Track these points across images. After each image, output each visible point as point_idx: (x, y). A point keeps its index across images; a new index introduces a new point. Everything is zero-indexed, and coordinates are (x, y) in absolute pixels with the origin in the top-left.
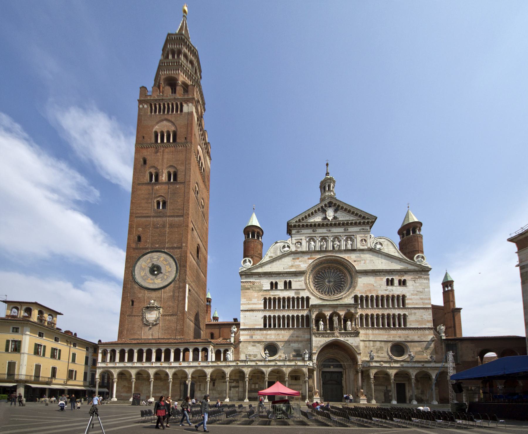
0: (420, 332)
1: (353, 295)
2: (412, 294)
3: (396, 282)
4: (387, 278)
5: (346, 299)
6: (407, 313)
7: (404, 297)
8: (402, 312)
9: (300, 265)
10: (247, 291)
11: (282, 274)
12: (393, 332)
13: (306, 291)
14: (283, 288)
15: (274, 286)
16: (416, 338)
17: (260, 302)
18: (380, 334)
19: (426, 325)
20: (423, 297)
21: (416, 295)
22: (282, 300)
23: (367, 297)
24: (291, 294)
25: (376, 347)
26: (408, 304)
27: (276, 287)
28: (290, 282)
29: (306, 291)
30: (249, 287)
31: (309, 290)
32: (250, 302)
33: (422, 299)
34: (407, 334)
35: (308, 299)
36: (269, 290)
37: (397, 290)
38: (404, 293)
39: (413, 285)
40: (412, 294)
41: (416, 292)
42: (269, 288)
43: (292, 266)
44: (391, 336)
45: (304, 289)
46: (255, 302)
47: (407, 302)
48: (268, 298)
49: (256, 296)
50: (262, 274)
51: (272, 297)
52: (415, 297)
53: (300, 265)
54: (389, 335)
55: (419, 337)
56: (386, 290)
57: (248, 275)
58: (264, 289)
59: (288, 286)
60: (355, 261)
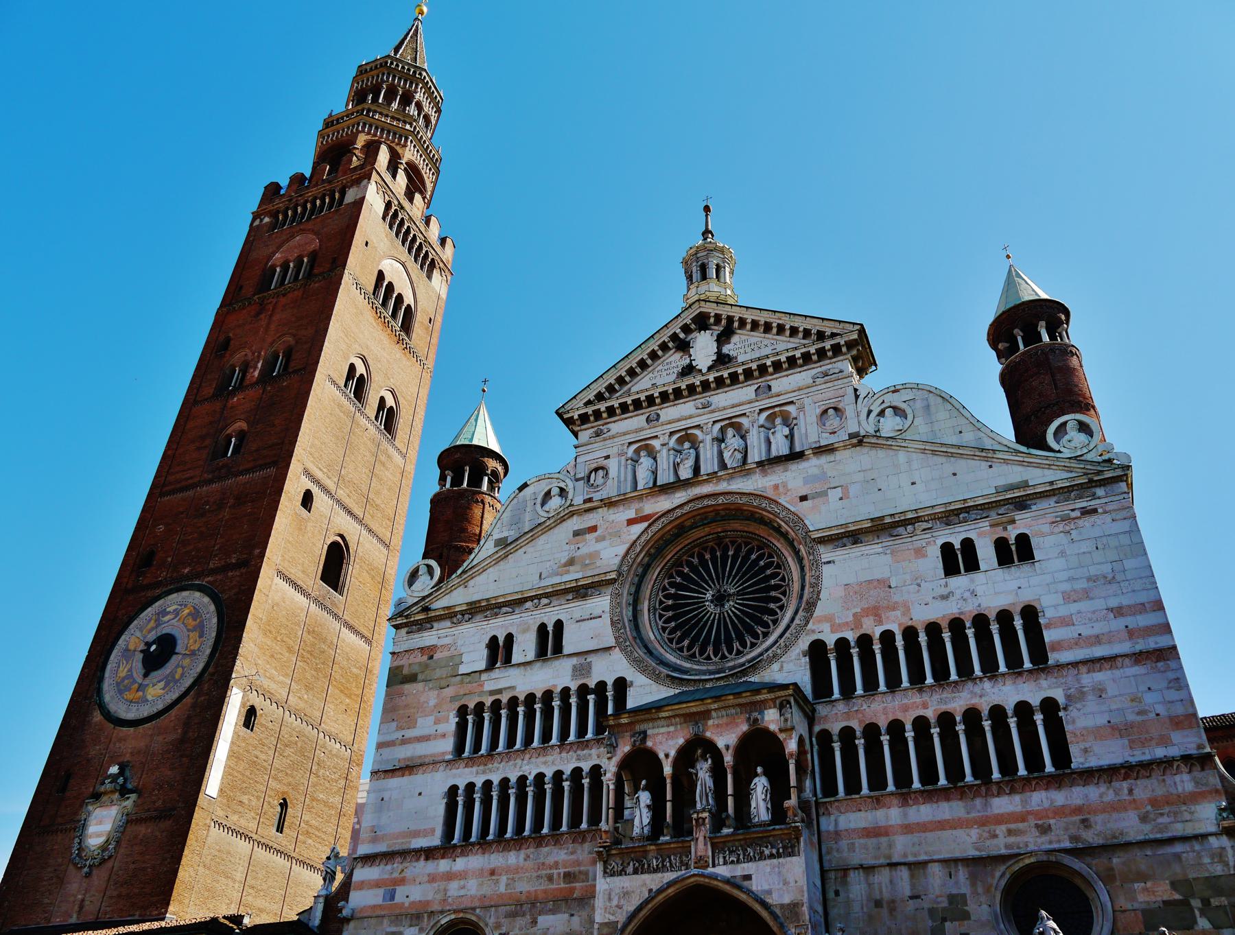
0: (1145, 789)
1: (804, 643)
2: (1068, 598)
3: (986, 553)
4: (940, 542)
5: (776, 666)
6: (1059, 695)
7: (1030, 613)
8: (1032, 692)
10: (407, 686)
11: (531, 598)
12: (1003, 804)
14: (531, 656)
15: (499, 652)
16: (1131, 826)
18: (941, 825)
19: (1165, 741)
20: (1126, 601)
21: (1086, 595)
22: (521, 709)
23: (865, 641)
24: (556, 676)
25: (926, 905)
26: (1058, 646)
27: (508, 660)
28: (559, 625)
29: (617, 654)
30: (416, 669)
33: (1118, 612)
34: (1078, 810)
35: (621, 685)
36: (481, 672)
37: (993, 590)
38: (1027, 597)
39: (1062, 554)
42: (482, 665)
43: (571, 562)
44: (1001, 830)
45: (608, 649)
46: (426, 732)
47: (1049, 636)
48: (471, 706)
49: (432, 703)
50: (463, 613)
51: (488, 701)
52: (1084, 606)
54: (982, 822)
55: (1144, 819)
56: (945, 597)
57: (416, 623)
58: (463, 669)
59: (550, 642)
60: (803, 498)
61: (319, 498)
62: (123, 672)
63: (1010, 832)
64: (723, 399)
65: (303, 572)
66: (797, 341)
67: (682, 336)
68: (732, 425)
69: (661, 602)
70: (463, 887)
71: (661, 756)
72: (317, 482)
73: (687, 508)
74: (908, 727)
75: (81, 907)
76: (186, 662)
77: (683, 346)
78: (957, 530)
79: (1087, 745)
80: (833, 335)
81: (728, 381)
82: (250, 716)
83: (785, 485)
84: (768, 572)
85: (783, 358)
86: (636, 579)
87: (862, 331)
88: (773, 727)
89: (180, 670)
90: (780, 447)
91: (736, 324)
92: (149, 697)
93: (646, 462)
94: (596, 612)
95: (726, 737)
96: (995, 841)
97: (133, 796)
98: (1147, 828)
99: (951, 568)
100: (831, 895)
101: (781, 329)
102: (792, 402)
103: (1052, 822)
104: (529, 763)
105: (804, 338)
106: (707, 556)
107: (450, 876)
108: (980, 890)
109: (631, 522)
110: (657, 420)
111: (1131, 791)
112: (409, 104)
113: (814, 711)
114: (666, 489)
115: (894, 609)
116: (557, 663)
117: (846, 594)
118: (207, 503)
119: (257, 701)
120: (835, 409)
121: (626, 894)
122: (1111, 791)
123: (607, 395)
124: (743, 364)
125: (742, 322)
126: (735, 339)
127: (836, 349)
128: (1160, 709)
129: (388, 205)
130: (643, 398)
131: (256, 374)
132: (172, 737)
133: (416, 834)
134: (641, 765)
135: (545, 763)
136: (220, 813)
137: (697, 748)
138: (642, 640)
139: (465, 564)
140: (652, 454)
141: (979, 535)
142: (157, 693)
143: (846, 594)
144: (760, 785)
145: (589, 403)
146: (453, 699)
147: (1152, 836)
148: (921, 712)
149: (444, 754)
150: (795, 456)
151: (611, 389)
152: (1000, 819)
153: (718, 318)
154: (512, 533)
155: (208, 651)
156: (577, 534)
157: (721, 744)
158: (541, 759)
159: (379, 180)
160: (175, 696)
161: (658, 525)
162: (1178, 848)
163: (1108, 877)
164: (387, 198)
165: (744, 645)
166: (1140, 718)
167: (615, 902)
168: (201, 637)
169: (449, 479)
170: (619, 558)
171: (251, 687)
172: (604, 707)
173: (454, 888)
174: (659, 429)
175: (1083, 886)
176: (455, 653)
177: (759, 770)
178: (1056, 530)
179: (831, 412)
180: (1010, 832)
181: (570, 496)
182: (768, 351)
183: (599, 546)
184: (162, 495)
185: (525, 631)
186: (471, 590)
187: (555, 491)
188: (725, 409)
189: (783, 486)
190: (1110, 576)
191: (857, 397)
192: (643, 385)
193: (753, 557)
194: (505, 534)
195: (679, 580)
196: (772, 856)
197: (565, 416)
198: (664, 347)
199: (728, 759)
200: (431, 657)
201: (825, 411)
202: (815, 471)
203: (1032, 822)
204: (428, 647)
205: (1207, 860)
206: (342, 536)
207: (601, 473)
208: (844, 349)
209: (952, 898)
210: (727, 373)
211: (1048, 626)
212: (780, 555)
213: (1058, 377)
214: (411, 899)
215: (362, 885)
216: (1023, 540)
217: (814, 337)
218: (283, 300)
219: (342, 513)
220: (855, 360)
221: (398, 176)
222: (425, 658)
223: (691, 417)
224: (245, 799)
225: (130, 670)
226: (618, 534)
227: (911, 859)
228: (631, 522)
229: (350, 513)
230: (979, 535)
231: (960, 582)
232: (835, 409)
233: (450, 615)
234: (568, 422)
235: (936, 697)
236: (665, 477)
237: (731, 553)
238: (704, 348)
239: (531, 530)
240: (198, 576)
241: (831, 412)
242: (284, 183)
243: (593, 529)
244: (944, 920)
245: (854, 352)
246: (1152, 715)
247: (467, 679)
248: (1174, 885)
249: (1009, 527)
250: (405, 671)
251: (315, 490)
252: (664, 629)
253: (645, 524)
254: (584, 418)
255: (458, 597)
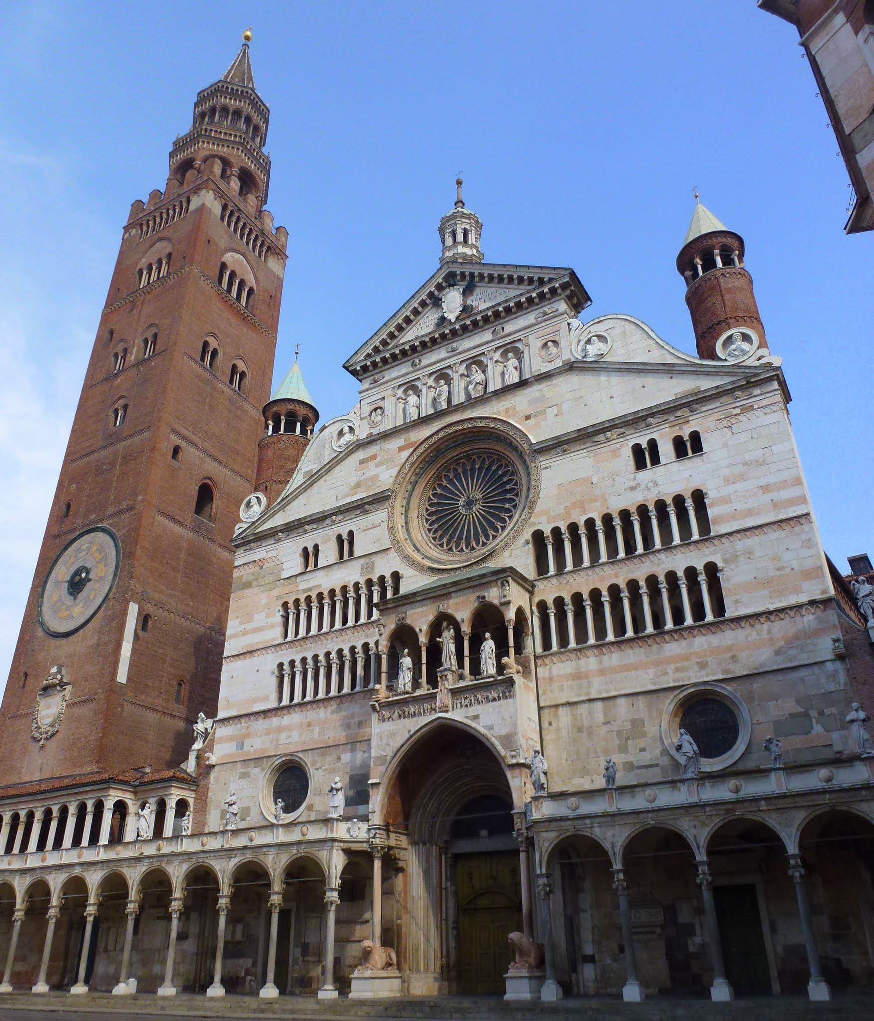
1: (528, 535)
2: (728, 480)
3: (666, 450)
4: (631, 443)
7: (699, 496)
8: (698, 559)
9: (377, 475)
10: (246, 591)
12: (673, 648)
13: (392, 554)
17: (271, 621)
18: (626, 668)
19: (797, 590)
20: (772, 479)
21: (742, 477)
23: (573, 528)
24: (350, 574)
25: (615, 729)
26: (719, 520)
28: (351, 534)
29: (392, 554)
30: (251, 578)
31: (399, 550)
32: (249, 626)
33: (766, 488)
34: (729, 648)
35: (396, 576)
37: (671, 478)
39: (725, 445)
40: (728, 480)
41: (740, 468)
43: (358, 485)
44: (671, 668)
47: (711, 512)
49: (264, 602)
52: (740, 486)
53: (377, 475)
54: (657, 664)
56: (633, 488)
58: (285, 575)
60: (528, 418)
61: (189, 452)
62: (56, 598)
63: (677, 669)
64: (467, 343)
65: (179, 509)
66: (524, 288)
67: (436, 293)
68: (475, 363)
69: (427, 510)
70: (289, 737)
71: (417, 630)
72: (184, 438)
73: (442, 434)
74: (605, 593)
75: (41, 769)
76: (97, 586)
77: (436, 301)
78: (643, 433)
79: (738, 597)
80: (551, 280)
81: (471, 327)
82: (144, 620)
83: (514, 408)
84: (505, 479)
85: (512, 304)
86: (406, 495)
87: (573, 274)
88: (496, 602)
89: (93, 593)
90: (513, 377)
91: (477, 279)
92: (75, 615)
93: (412, 399)
94: (377, 523)
95: (463, 610)
96: (666, 678)
97: (69, 688)
98: (779, 658)
99: (640, 464)
100: (545, 725)
101: (511, 279)
102: (520, 340)
103: (709, 659)
104: (332, 642)
105: (529, 284)
106: (460, 471)
107: (280, 730)
108: (654, 715)
109: (401, 449)
110: (419, 364)
111: (769, 631)
112: (240, 117)
113: (533, 586)
114: (423, 421)
115: (595, 500)
116: (350, 564)
117: (562, 491)
118: (104, 464)
119: (149, 608)
120: (554, 342)
121: (392, 735)
122: (754, 632)
123: (381, 348)
124: (481, 312)
125: (481, 276)
126: (478, 291)
127: (553, 291)
128: (795, 564)
129: (225, 207)
130: (407, 348)
131: (133, 358)
132: (93, 641)
133: (256, 700)
134: (403, 637)
135: (343, 641)
136: (131, 695)
137: (442, 621)
138: (411, 541)
139: (283, 494)
140: (417, 392)
141: (662, 436)
142: (80, 610)
143: (562, 491)
144: (489, 646)
145: (368, 356)
146: (278, 598)
147: (784, 666)
148: (614, 581)
149: (273, 639)
150: (523, 384)
151: (384, 343)
152: (670, 660)
153: (463, 274)
154: (316, 466)
155: (111, 577)
156: (362, 462)
157: (459, 618)
158: (341, 638)
159: (214, 187)
160: (91, 612)
161: (421, 449)
162: (803, 673)
163: (750, 699)
164: (224, 202)
165: (487, 538)
166: (779, 573)
167: (384, 742)
168: (106, 566)
169: (271, 428)
170: (393, 478)
171: (142, 601)
172: (386, 595)
173: (283, 738)
174: (420, 372)
175: (732, 707)
176: (278, 563)
177: (488, 635)
178: (721, 426)
179: (550, 344)
180: (677, 669)
181: (356, 433)
182: (502, 298)
183: (379, 469)
184: (73, 461)
185: (326, 542)
186: (289, 513)
187: (346, 429)
188: (469, 350)
189: (510, 411)
190: (761, 460)
191: (570, 329)
192: (409, 336)
193: (494, 468)
194: (311, 467)
195: (439, 491)
196: (494, 700)
197: (350, 369)
198: (423, 304)
199: (466, 628)
200: (262, 567)
201: (545, 345)
202: (538, 394)
203: (694, 659)
204: (260, 560)
205: (823, 680)
206: (210, 478)
207: (379, 411)
208: (559, 291)
209: (634, 722)
210: (472, 323)
211: (712, 505)
212: (512, 464)
213: (727, 297)
214: (255, 747)
215: (222, 740)
216: (696, 437)
217: (536, 283)
218: (149, 297)
219: (208, 460)
220: (569, 298)
221: (233, 184)
222: (258, 568)
223: (443, 360)
224: (149, 683)
225: (60, 596)
226: (391, 460)
227: (604, 695)
228: (401, 449)
229: (215, 459)
230: (662, 436)
231: (648, 474)
232: (554, 342)
233: (273, 534)
234: (354, 373)
235: (625, 569)
236: (428, 411)
237: (477, 466)
238: (453, 301)
239: (328, 463)
240: (101, 521)
241: (550, 344)
242: (145, 199)
243: (374, 457)
244: (628, 739)
245: (568, 292)
246: (788, 570)
247: (289, 581)
248: (798, 702)
249: (684, 427)
250: (244, 580)
251: (183, 444)
252: (429, 530)
253: (412, 449)
254: (365, 369)
255: (279, 520)
